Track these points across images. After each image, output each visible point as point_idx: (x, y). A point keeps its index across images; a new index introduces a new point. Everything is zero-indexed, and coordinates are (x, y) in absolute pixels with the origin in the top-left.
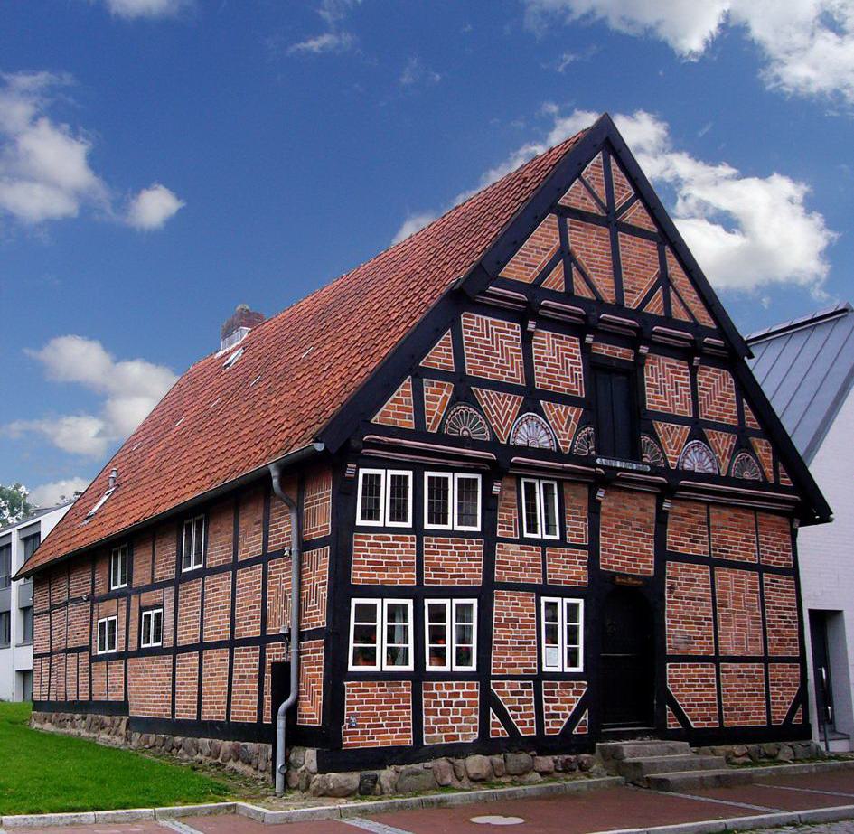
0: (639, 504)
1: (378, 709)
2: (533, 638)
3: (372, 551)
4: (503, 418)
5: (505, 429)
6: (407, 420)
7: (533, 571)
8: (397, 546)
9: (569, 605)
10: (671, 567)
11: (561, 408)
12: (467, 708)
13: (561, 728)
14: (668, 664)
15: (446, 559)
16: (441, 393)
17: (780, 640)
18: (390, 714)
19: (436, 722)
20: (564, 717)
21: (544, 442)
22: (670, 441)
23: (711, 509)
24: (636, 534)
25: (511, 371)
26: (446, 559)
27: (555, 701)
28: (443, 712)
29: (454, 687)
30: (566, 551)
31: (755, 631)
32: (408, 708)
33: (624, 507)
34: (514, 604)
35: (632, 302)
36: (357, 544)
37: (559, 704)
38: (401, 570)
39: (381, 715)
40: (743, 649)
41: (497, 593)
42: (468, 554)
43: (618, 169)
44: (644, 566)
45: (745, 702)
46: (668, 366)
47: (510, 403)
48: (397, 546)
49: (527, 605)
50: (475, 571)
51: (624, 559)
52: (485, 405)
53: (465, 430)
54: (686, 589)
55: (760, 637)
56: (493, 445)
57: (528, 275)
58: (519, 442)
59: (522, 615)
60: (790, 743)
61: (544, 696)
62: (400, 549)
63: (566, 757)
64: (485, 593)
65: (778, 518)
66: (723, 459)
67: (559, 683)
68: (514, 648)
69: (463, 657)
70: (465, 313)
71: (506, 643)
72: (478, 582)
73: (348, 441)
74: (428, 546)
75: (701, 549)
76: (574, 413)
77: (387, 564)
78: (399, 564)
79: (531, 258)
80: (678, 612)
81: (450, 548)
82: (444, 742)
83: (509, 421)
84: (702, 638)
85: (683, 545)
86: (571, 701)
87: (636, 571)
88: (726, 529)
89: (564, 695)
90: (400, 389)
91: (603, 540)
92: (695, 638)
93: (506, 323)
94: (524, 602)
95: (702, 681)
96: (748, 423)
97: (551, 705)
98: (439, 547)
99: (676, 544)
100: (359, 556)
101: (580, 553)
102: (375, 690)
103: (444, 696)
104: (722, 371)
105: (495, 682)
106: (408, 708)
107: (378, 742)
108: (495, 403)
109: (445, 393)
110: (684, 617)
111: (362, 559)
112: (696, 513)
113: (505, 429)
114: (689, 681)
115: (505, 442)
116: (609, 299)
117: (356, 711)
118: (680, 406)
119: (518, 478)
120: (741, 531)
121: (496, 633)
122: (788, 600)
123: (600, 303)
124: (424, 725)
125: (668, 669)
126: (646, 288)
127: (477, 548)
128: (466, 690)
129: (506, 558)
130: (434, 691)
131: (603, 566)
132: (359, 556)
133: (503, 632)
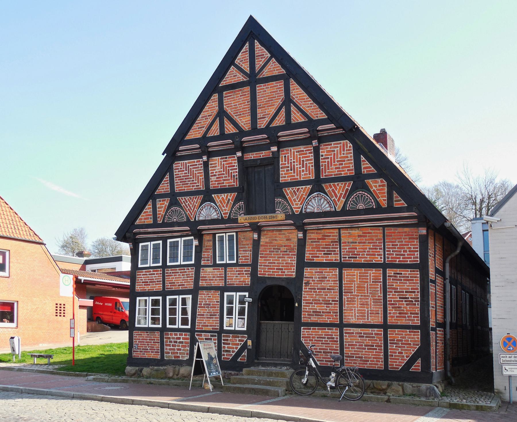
0: (285, 237)
1: (146, 342)
2: (218, 313)
3: (144, 277)
4: (192, 209)
5: (193, 214)
6: (150, 220)
7: (219, 280)
8: (154, 274)
9: (182, 298)
10: (307, 272)
11: (224, 196)
12: (184, 344)
13: (231, 358)
14: (302, 328)
15: (176, 278)
16: (163, 204)
17: (399, 313)
18: (151, 345)
19: (170, 349)
20: (233, 352)
21: (214, 215)
22: (295, 197)
23: (342, 232)
24: (283, 255)
25: (197, 184)
26: (176, 278)
27: (229, 344)
28: (173, 346)
29: (178, 334)
30: (238, 269)
31: (376, 308)
32: (158, 343)
33: (276, 240)
34: (208, 297)
35: (262, 124)
36: (138, 275)
37: (231, 346)
38: (156, 284)
39: (147, 345)
40: (364, 319)
41: (200, 292)
42: (186, 275)
43: (260, 46)
44: (288, 272)
45: (363, 353)
46: (298, 152)
47: (196, 200)
48: (154, 274)
49: (215, 297)
50: (190, 282)
51: (274, 269)
52: (184, 204)
53: (174, 219)
54: (319, 284)
55: (381, 311)
56: (188, 223)
57: (199, 133)
58: (201, 218)
59: (213, 302)
60: (401, 383)
61: (223, 341)
62: (156, 275)
63: (230, 372)
64: (195, 292)
65: (406, 229)
66: (339, 200)
67: (231, 335)
68: (207, 318)
69: (185, 321)
70: (176, 162)
71: (203, 315)
72: (191, 287)
73: (125, 235)
74: (167, 273)
75: (334, 258)
76: (231, 196)
77: (150, 282)
78: (155, 282)
79: (202, 123)
80: (312, 297)
81: (178, 272)
82: (173, 359)
83: (195, 209)
84: (330, 313)
85: (319, 257)
86: (238, 344)
87: (283, 275)
88: (356, 243)
89: (234, 341)
90: (147, 207)
91: (260, 260)
92: (323, 312)
93: (196, 160)
94: (215, 296)
95: (327, 338)
96: (364, 171)
97: (226, 346)
98: (173, 273)
99: (312, 257)
100: (139, 280)
101: (246, 268)
102: (145, 335)
103: (173, 338)
104: (342, 142)
105: (197, 333)
106: (158, 343)
107: (146, 356)
108: (188, 202)
109: (166, 203)
110: (316, 300)
111: (140, 281)
112: (330, 236)
113: (193, 214)
114: (317, 338)
115: (193, 220)
116: (247, 128)
117: (137, 343)
118: (305, 174)
119: (214, 235)
120: (369, 243)
121: (199, 310)
122: (411, 286)
123: (242, 133)
124: (165, 351)
125: (302, 330)
126: (272, 111)
127: (191, 272)
128: (183, 336)
129: (206, 274)
130: (169, 336)
131: (260, 274)
132: (139, 280)
133: (203, 310)
